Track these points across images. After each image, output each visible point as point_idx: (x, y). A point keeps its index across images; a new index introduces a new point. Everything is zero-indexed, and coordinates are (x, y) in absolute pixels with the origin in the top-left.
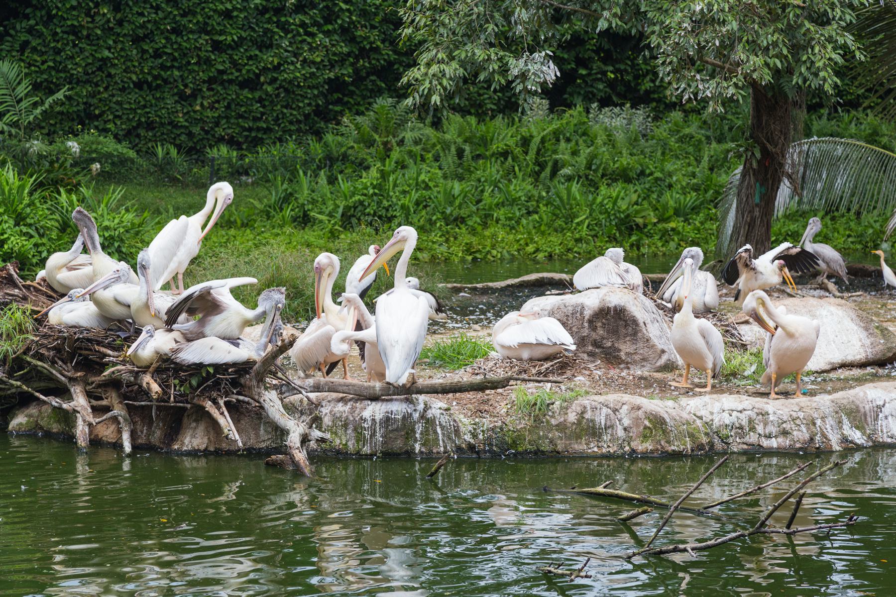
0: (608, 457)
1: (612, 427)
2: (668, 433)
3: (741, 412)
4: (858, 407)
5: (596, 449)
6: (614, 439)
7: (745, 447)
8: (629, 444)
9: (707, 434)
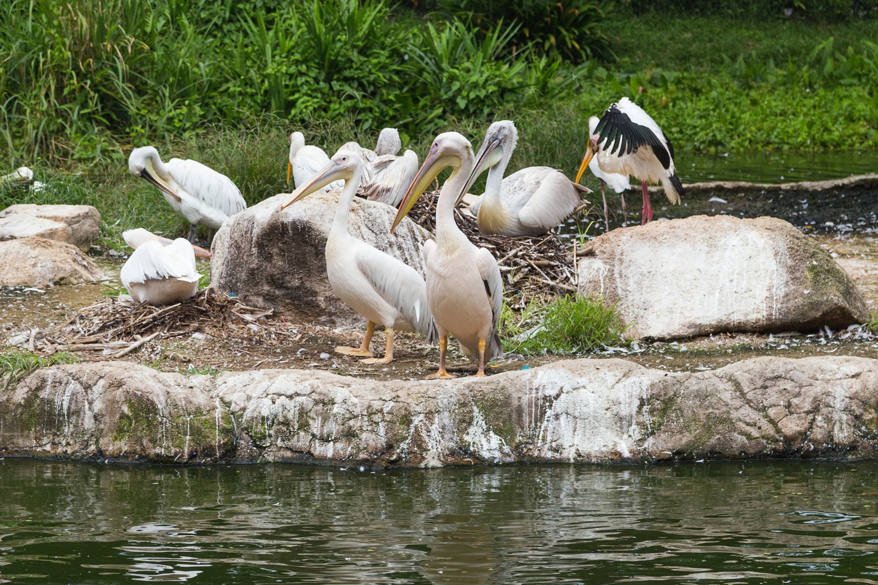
0: (65, 459)
1: (78, 413)
2: (155, 426)
3: (291, 397)
4: (508, 397)
5: (48, 448)
6: (79, 432)
7: (289, 454)
8: (97, 442)
9: (226, 432)
